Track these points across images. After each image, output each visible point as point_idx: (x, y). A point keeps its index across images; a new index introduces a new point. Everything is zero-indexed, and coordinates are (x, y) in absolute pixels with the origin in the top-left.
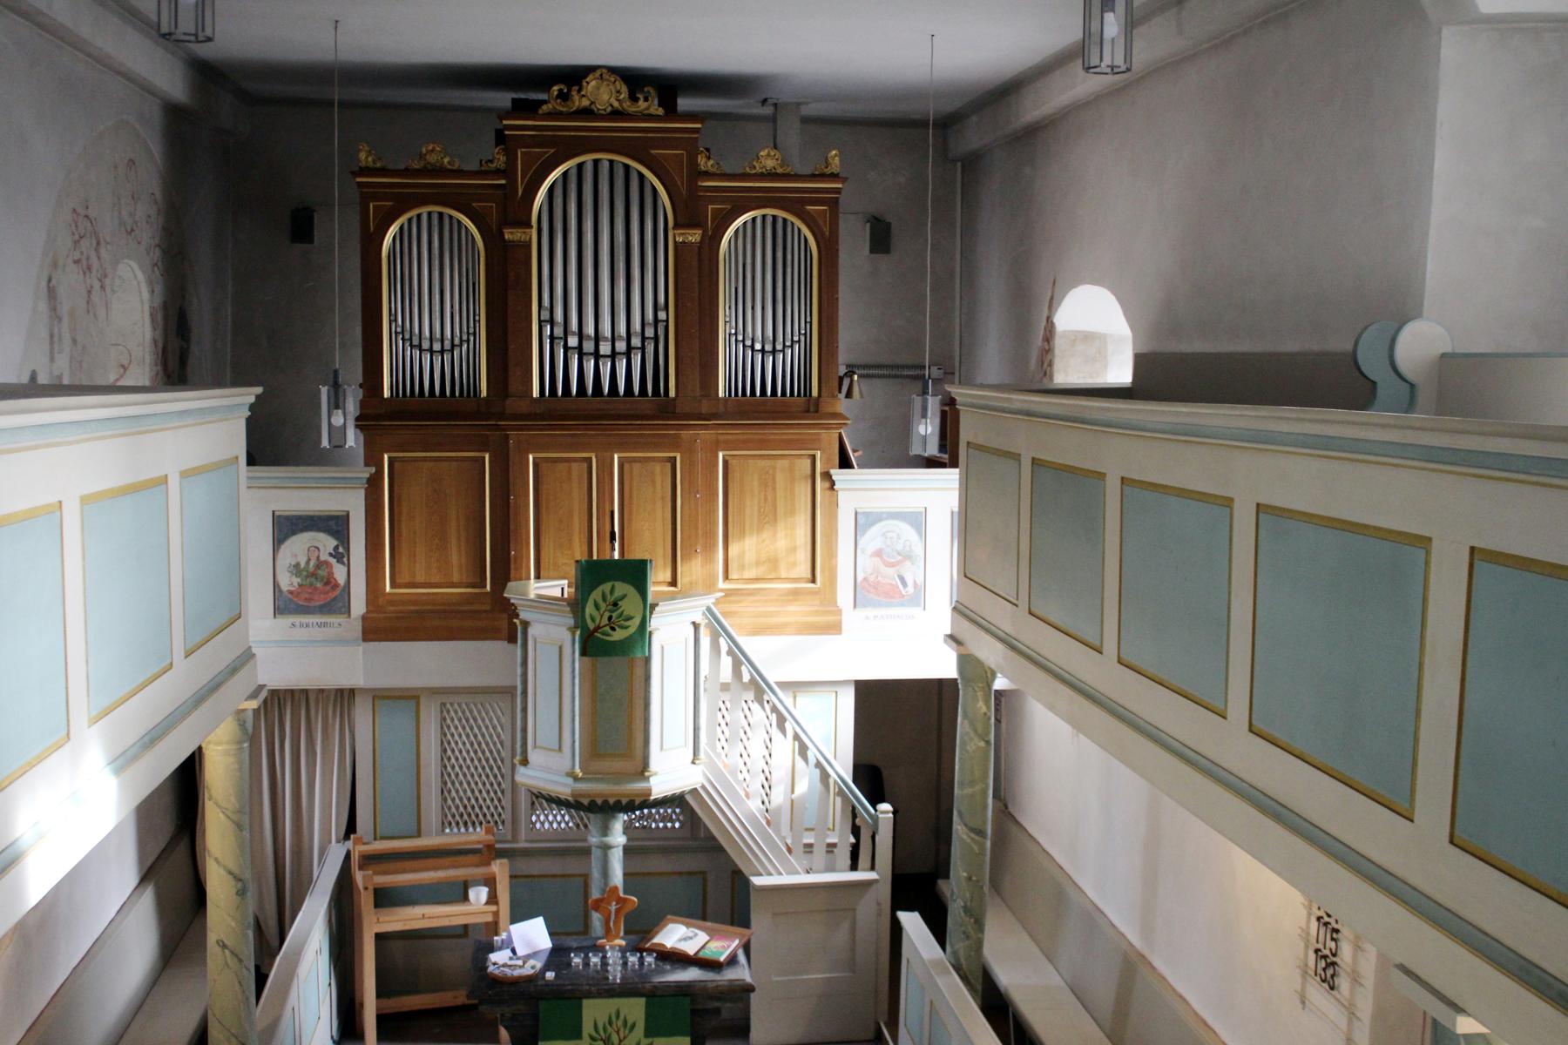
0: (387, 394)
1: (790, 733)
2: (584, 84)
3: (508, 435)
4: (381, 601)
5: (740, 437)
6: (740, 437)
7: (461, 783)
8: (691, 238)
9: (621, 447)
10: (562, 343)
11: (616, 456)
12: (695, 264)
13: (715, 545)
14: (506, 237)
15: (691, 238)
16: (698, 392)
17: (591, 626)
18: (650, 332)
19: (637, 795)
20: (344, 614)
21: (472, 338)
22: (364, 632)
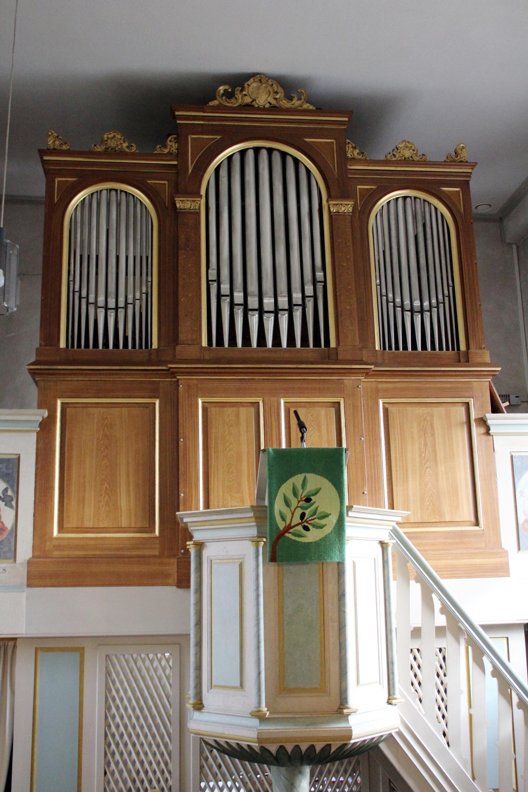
0: (62, 344)
1: (489, 668)
2: (246, 85)
3: (178, 379)
4: (48, 545)
5: (398, 385)
6: (398, 385)
7: (126, 745)
8: (343, 209)
9: (287, 393)
10: (228, 299)
11: (282, 402)
12: (349, 230)
13: (380, 488)
14: (178, 206)
15: (343, 209)
16: (357, 343)
17: (282, 525)
18: (309, 290)
19: (335, 739)
20: (9, 559)
21: (144, 296)
22: (29, 578)
